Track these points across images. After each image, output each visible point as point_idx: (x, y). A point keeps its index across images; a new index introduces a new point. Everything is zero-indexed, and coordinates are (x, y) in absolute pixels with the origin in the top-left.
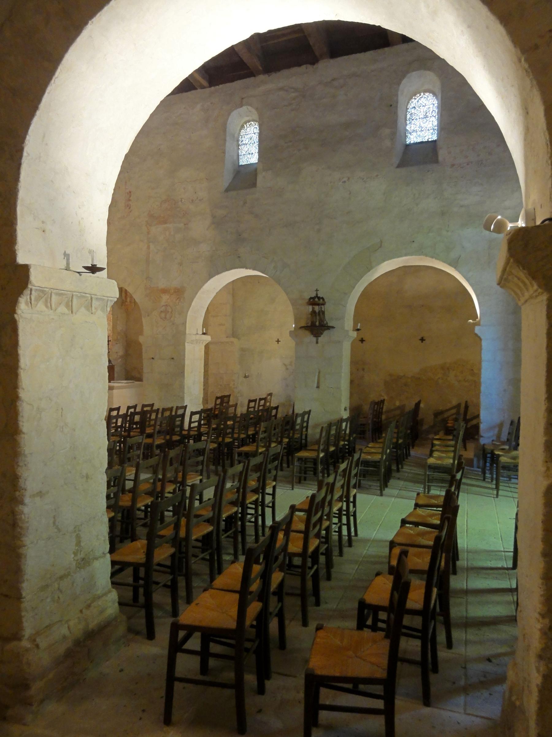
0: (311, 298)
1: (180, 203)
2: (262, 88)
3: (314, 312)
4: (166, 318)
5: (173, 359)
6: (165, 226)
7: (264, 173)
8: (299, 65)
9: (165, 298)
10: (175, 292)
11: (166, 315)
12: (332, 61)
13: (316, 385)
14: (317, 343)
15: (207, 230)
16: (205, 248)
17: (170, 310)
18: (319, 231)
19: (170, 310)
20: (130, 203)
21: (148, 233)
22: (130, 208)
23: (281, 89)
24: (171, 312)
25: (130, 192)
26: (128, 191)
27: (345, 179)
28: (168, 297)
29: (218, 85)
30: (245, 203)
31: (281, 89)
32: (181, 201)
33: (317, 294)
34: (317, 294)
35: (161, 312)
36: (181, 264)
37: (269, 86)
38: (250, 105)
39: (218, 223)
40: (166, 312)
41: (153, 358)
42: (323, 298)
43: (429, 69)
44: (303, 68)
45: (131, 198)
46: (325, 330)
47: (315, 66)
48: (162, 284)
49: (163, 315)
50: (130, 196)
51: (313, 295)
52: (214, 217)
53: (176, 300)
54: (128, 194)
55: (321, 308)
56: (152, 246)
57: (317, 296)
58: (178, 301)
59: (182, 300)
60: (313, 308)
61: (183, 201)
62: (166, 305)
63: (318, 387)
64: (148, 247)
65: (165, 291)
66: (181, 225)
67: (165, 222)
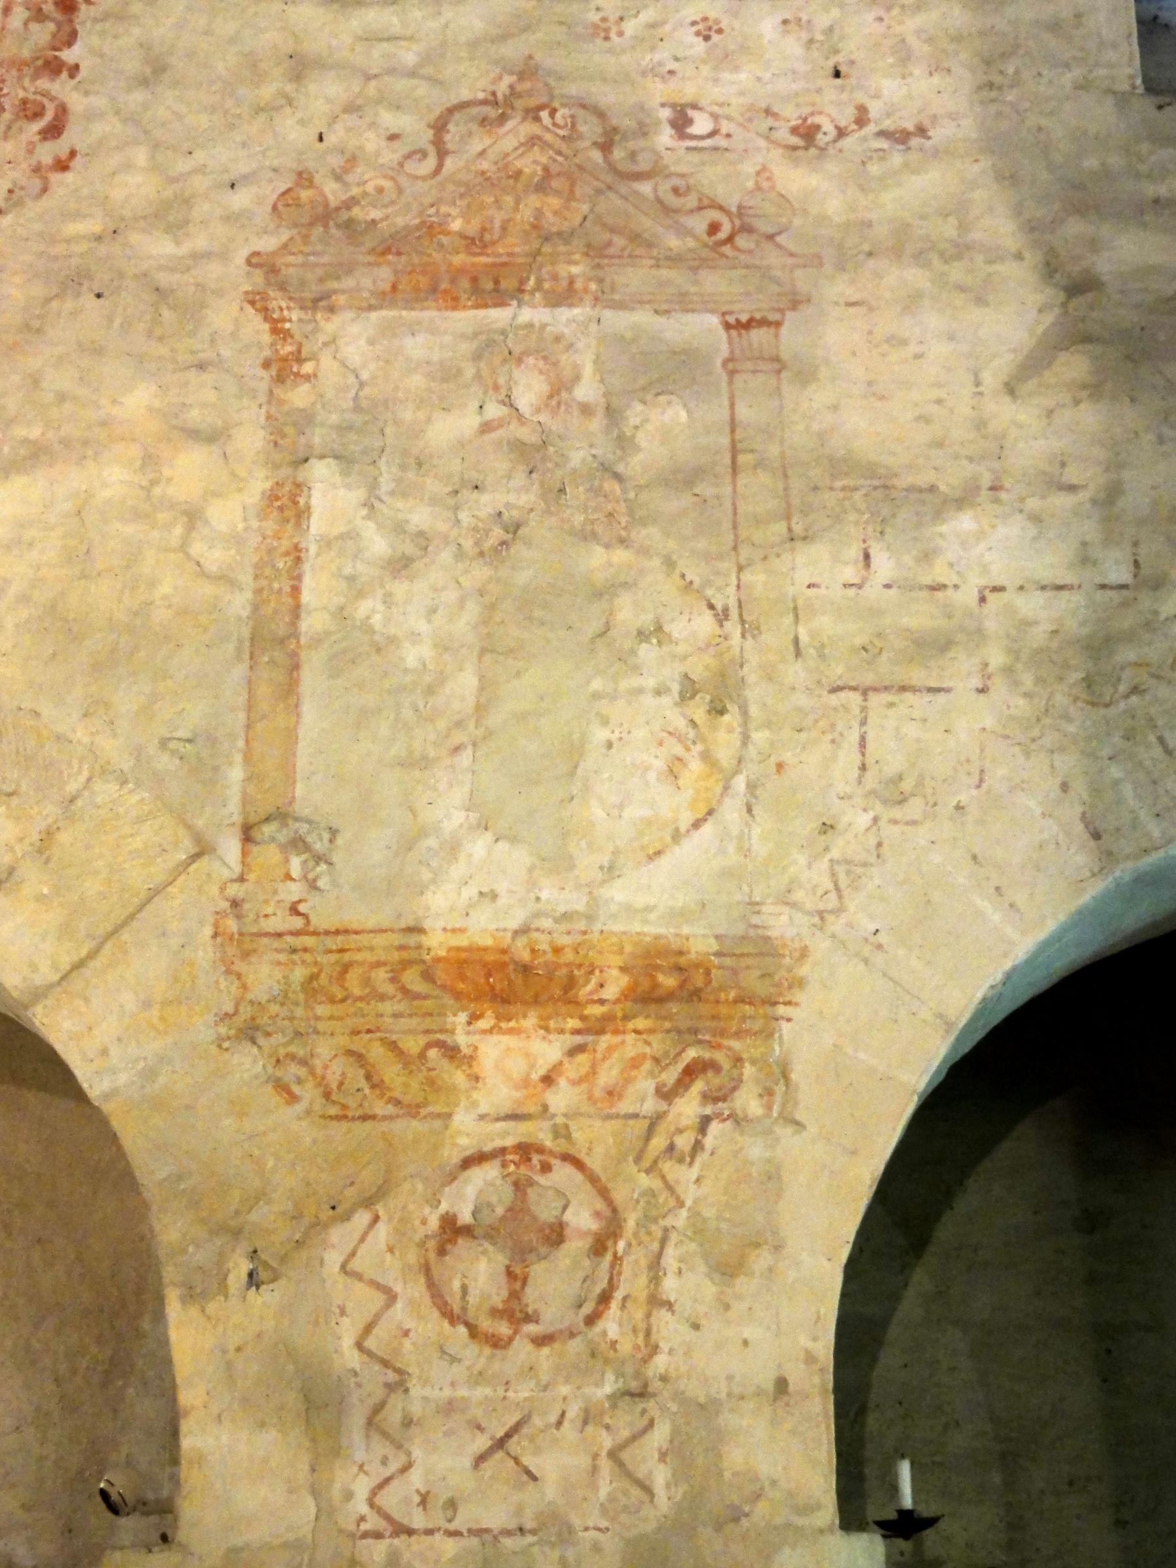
1: (665, 137)
4: (515, 1312)
6: (498, 316)
9: (507, 1058)
10: (644, 997)
11: (516, 1279)
15: (1010, 390)
17: (582, 1218)
19: (582, 1218)
20: (61, 87)
21: (285, 368)
22: (54, 131)
24: (599, 1247)
28: (548, 1051)
32: (681, 123)
40: (526, 1237)
45: (68, 55)
48: (475, 896)
49: (480, 1273)
53: (667, 1095)
56: (330, 496)
58: (688, 1107)
59: (748, 1101)
61: (701, 125)
62: (525, 1150)
64: (288, 504)
65: (510, 982)
66: (702, 328)
67: (493, 286)
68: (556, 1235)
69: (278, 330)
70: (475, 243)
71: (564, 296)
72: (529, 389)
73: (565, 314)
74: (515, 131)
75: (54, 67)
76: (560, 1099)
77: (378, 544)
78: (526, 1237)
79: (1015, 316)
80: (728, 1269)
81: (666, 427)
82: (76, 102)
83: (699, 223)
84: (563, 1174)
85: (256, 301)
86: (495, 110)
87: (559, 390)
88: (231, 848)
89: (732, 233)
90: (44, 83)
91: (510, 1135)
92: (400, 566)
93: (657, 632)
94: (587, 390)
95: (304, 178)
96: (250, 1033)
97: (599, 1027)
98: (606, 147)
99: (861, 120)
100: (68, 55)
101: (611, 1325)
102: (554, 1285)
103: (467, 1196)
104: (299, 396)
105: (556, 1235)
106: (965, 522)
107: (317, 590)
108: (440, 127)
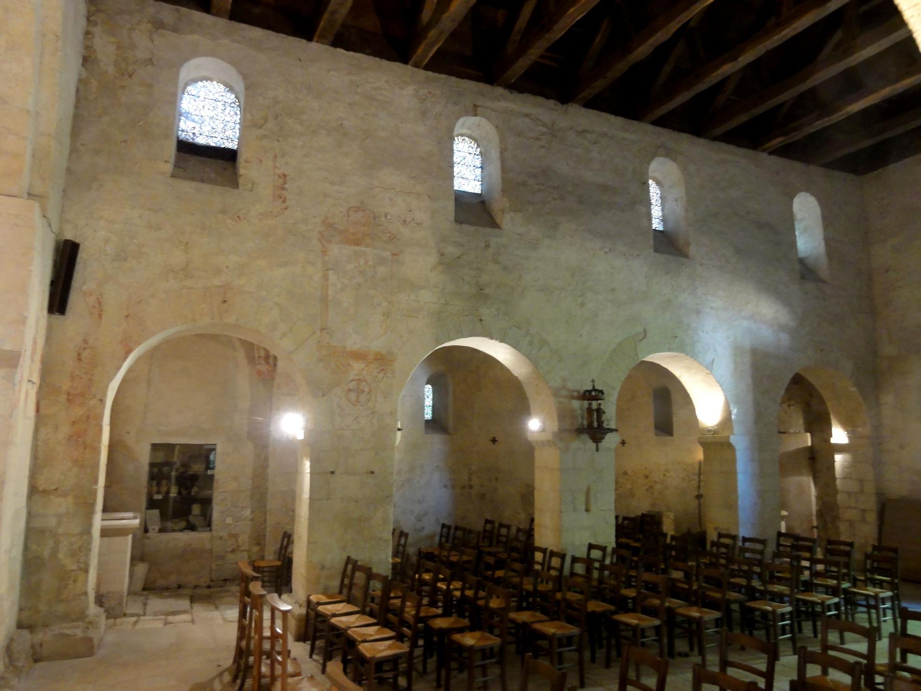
0: (587, 391)
1: (383, 219)
2: (502, 104)
3: (590, 410)
4: (358, 401)
5: (372, 472)
6: (358, 248)
7: (512, 214)
8: (548, 97)
10: (376, 359)
11: (358, 397)
12: (583, 111)
13: (583, 507)
14: (597, 450)
15: (431, 270)
16: (427, 297)
17: (367, 389)
18: (582, 305)
19: (367, 389)
21: (324, 253)
22: (284, 201)
23: (527, 115)
24: (369, 393)
25: (285, 176)
26: (280, 172)
27: (607, 250)
28: (362, 366)
29: (440, 72)
30: (487, 246)
31: (527, 115)
32: (386, 216)
33: (594, 387)
34: (594, 387)
35: (349, 390)
36: (387, 315)
37: (512, 106)
38: (488, 119)
39: (448, 264)
40: (360, 392)
41: (332, 473)
42: (601, 392)
43: (674, 160)
44: (551, 103)
45: (286, 186)
46: (606, 433)
47: (565, 106)
48: (354, 343)
49: (353, 396)
50: (285, 183)
51: (590, 388)
52: (442, 255)
53: (379, 373)
54: (279, 177)
55: (600, 404)
56: (332, 276)
57: (594, 390)
58: (381, 375)
59: (389, 375)
60: (590, 404)
61: (389, 217)
62: (359, 380)
63: (587, 510)
64: (326, 278)
65: (359, 356)
66: (387, 254)
67: (357, 243)
68: (363, 391)
69: (323, 246)
70: (354, 234)
71: (367, 246)
72: (362, 262)
73: (368, 249)
74: (360, 214)
75: (283, 188)
76: (364, 373)
77: (339, 286)
78: (360, 392)
79: (433, 259)
80: (385, 397)
81: (382, 270)
82: (288, 197)
83: (388, 235)
84: (364, 383)
85: (320, 240)
86: (358, 209)
87: (366, 262)
88: (319, 333)
89: (393, 238)
90: (283, 192)
91: (357, 377)
92: (343, 290)
93: (379, 305)
94: (370, 263)
95: (327, 218)
96: (321, 360)
97: (370, 363)
98: (374, 219)
99: (413, 220)
100: (286, 186)
101: (370, 404)
102: (363, 398)
103: (352, 385)
104: (327, 258)
105: (363, 391)
106: (423, 292)
107: (331, 292)
108: (348, 211)
